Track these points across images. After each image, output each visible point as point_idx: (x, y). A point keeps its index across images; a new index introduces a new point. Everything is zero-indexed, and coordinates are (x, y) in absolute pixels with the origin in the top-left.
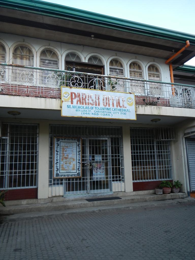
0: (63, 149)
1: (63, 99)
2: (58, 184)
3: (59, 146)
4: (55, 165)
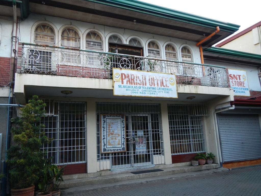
0: (109, 125)
2: (105, 158)
3: (106, 122)
4: (102, 140)
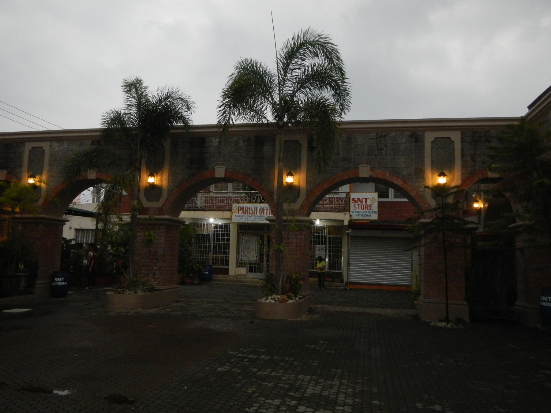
1: (233, 212)
2: (242, 266)
